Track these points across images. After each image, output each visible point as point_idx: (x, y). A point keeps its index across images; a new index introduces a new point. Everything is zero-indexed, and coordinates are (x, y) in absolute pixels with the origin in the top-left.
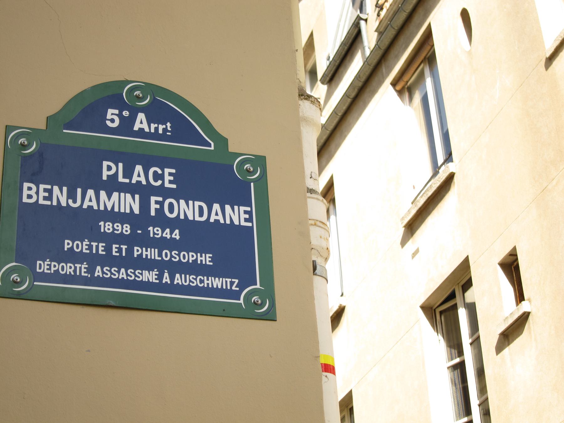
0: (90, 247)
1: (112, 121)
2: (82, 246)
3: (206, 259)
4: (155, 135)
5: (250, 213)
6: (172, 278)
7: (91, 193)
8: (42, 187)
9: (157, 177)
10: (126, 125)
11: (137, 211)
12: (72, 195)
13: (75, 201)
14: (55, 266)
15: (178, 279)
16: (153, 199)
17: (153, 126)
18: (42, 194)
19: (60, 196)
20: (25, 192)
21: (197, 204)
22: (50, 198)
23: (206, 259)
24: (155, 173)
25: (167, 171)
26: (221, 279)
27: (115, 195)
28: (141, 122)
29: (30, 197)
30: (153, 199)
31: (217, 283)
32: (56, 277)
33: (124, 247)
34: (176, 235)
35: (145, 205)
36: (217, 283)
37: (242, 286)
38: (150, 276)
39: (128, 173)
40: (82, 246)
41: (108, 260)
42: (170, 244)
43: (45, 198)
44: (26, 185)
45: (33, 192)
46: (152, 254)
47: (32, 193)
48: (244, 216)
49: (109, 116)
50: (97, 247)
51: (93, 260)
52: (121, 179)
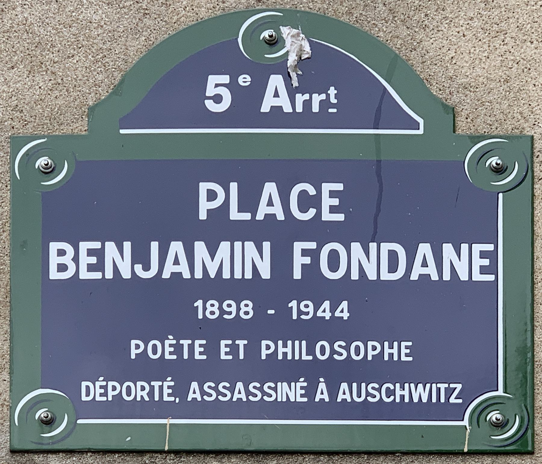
0: (178, 349)
1: (218, 99)
2: (164, 349)
3: (400, 351)
4: (306, 118)
5: (492, 256)
6: (333, 391)
7: (176, 247)
8: (84, 246)
9: (305, 201)
10: (246, 105)
11: (265, 273)
12: (141, 257)
13: (147, 268)
14: (114, 389)
15: (345, 393)
16: (298, 247)
17: (300, 98)
18: (85, 260)
19: (119, 259)
20: (54, 260)
21: (386, 247)
22: (99, 267)
23: (400, 351)
24: (303, 194)
25: (327, 187)
26: (428, 386)
27: (224, 247)
28: (276, 95)
29: (62, 268)
30: (298, 247)
31: (421, 393)
32: (118, 407)
33: (241, 343)
34: (343, 311)
35: (282, 260)
36: (421, 393)
37: (467, 396)
38: (292, 392)
39: (249, 202)
40: (164, 349)
41: (211, 370)
42: (331, 330)
43: (91, 268)
44: (54, 247)
45: (67, 259)
46: (294, 350)
47: (66, 261)
48: (478, 262)
49: (210, 91)
50: (191, 347)
51: (183, 372)
52: (235, 215)
